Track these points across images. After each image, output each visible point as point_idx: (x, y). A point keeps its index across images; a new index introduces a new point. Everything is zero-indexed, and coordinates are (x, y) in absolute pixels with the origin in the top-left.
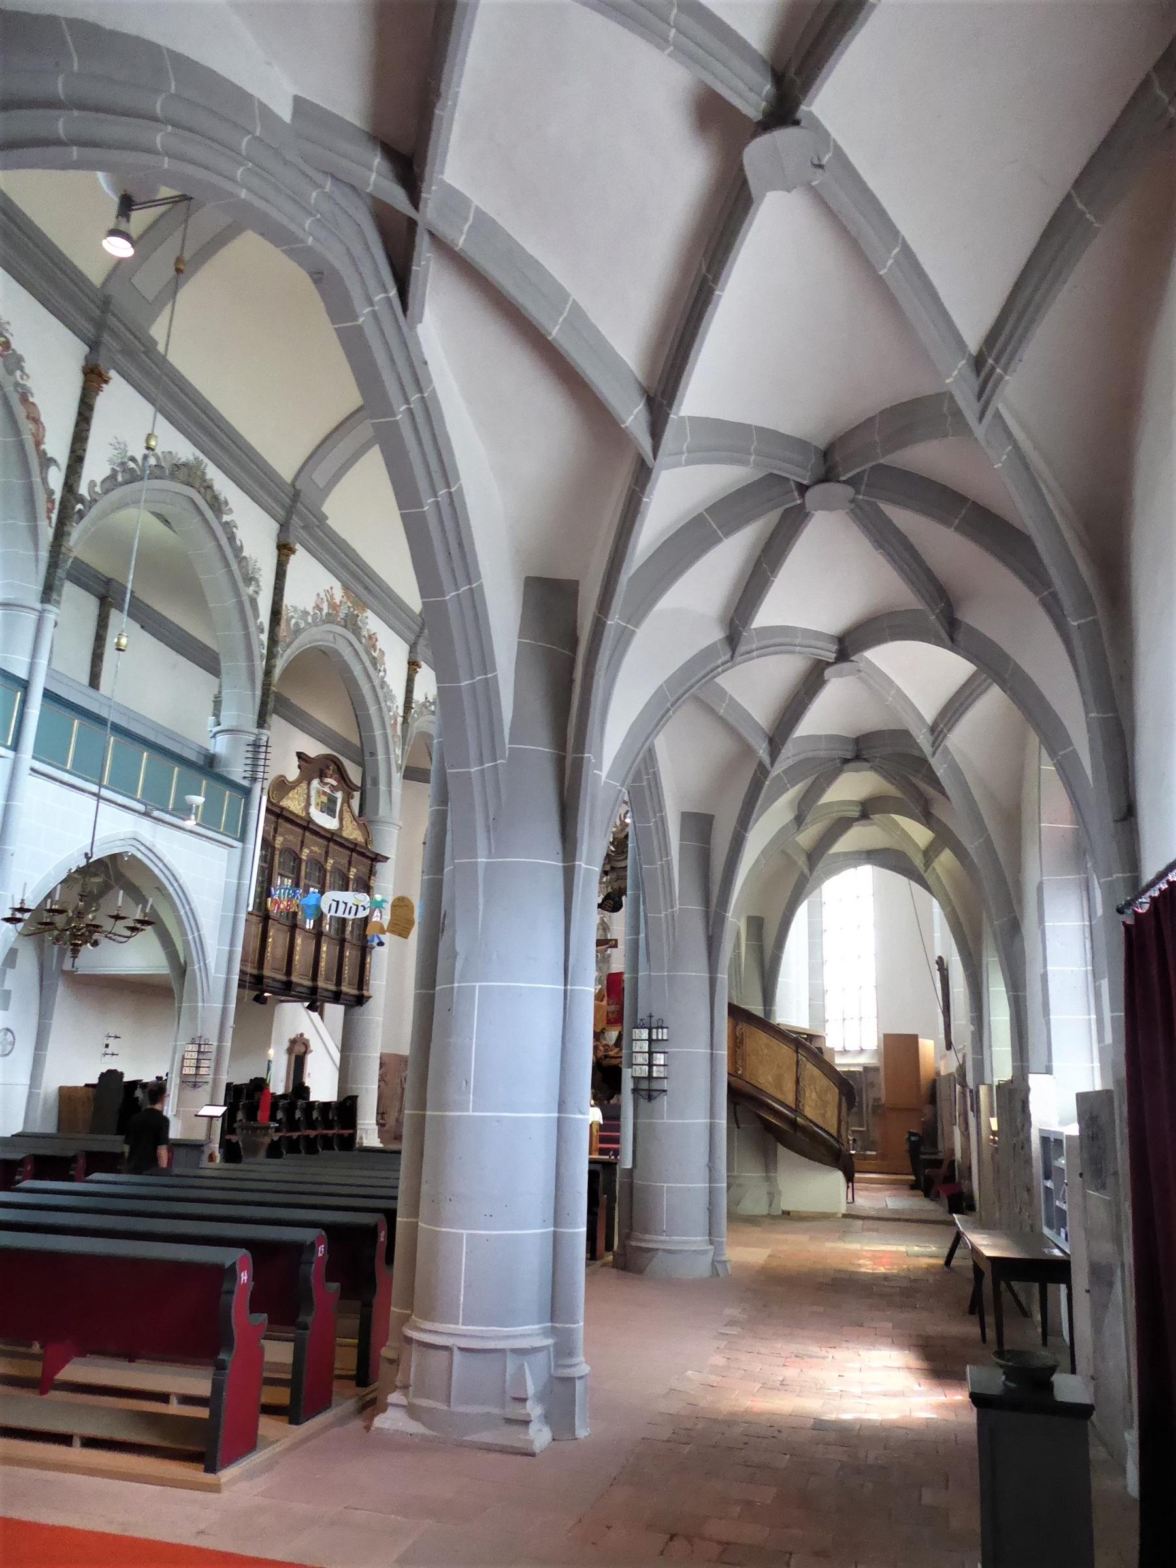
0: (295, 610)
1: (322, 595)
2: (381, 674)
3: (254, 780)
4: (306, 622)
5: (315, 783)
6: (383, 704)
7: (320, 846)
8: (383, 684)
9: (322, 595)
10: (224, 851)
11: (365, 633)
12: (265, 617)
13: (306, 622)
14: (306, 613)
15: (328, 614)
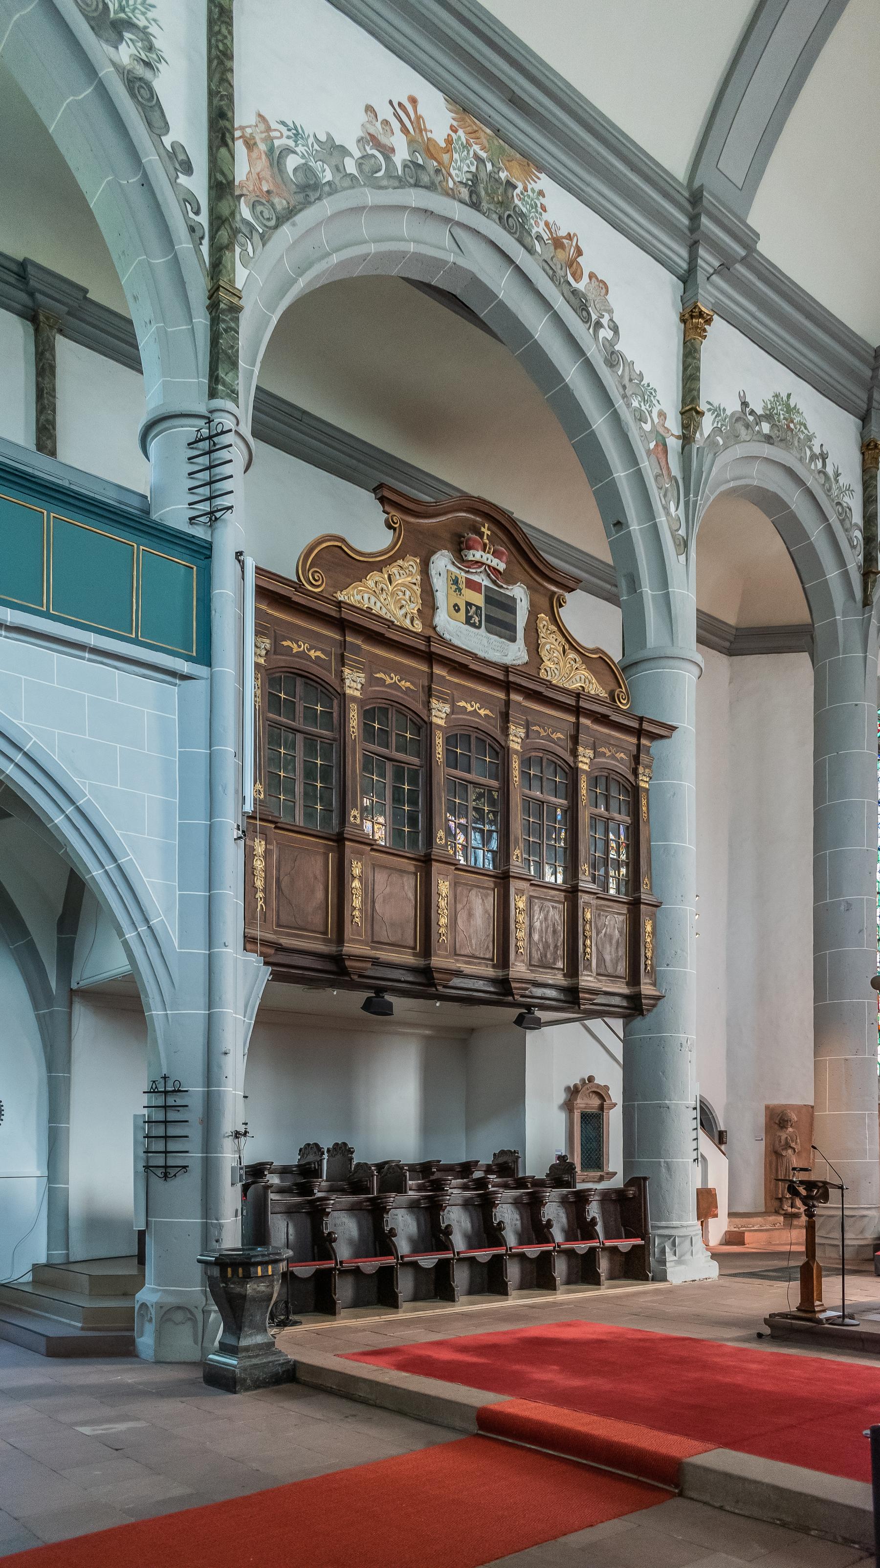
0: (297, 134)
1: (385, 112)
2: (605, 333)
3: (213, 518)
4: (338, 169)
5: (442, 562)
6: (619, 403)
7: (485, 701)
8: (613, 359)
9: (385, 112)
10: (173, 691)
11: (538, 228)
12: (186, 127)
13: (338, 169)
14: (333, 150)
15: (412, 166)
